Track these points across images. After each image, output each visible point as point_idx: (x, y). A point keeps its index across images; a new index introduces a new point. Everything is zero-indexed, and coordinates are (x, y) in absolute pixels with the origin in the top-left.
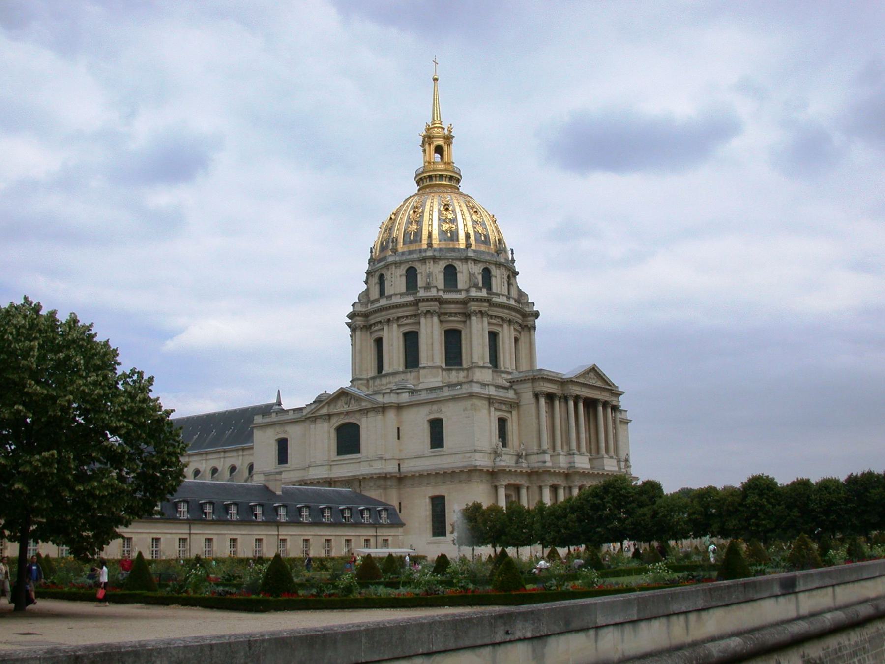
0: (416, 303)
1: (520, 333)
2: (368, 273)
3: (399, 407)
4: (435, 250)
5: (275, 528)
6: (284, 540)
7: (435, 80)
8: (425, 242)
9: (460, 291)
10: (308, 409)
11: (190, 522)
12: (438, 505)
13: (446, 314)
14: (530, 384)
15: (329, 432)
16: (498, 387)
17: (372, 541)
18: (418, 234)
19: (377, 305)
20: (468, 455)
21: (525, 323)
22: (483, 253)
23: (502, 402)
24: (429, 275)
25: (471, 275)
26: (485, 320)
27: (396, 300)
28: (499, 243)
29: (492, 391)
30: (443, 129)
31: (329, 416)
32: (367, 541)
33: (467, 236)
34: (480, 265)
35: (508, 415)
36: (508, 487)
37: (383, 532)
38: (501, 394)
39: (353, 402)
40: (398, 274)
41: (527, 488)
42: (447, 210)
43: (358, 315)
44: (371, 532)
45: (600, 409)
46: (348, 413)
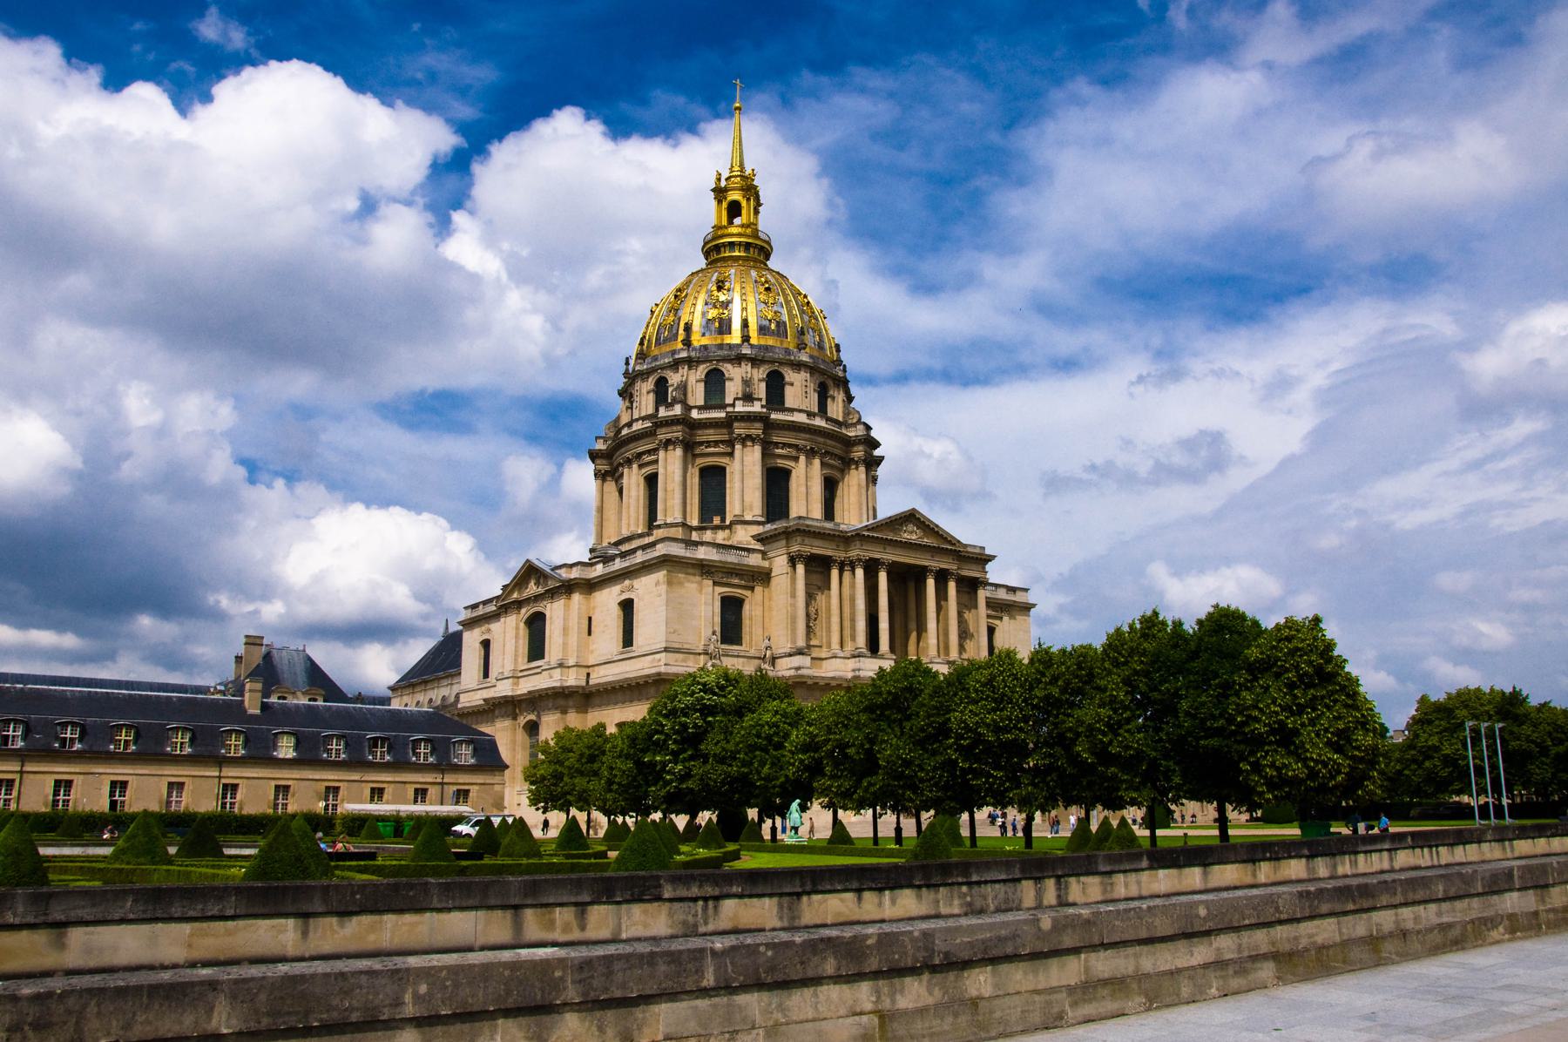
6: (235, 787)
8: (681, 335)
9: (723, 406)
11: (22, 756)
13: (701, 443)
17: (433, 792)
18: (673, 329)
22: (767, 348)
24: (683, 387)
26: (757, 449)
27: (637, 426)
33: (745, 324)
35: (747, 593)
40: (644, 391)
45: (931, 583)
46: (537, 598)
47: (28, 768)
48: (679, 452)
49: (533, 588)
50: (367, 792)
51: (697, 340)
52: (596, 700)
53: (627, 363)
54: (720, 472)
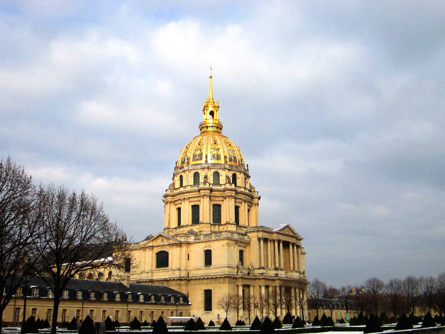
0: (199, 191)
2: (174, 175)
3: (188, 244)
4: (209, 164)
5: (126, 305)
6: (130, 311)
9: (221, 185)
10: (142, 243)
12: (208, 294)
16: (239, 234)
17: (175, 313)
18: (201, 155)
19: (178, 191)
20: (224, 269)
21: (253, 202)
23: (242, 242)
24: (206, 177)
25: (227, 177)
26: (233, 200)
27: (188, 189)
28: (241, 161)
29: (236, 236)
30: (214, 102)
31: (153, 247)
32: (172, 312)
33: (225, 157)
36: (244, 286)
37: (181, 308)
41: (254, 286)
43: (169, 196)
44: (174, 308)
45: (291, 247)
47: (84, 306)
48: (208, 199)
49: (159, 242)
50: (160, 312)
51: (210, 161)
52: (193, 282)
53: (176, 164)
54: (220, 206)
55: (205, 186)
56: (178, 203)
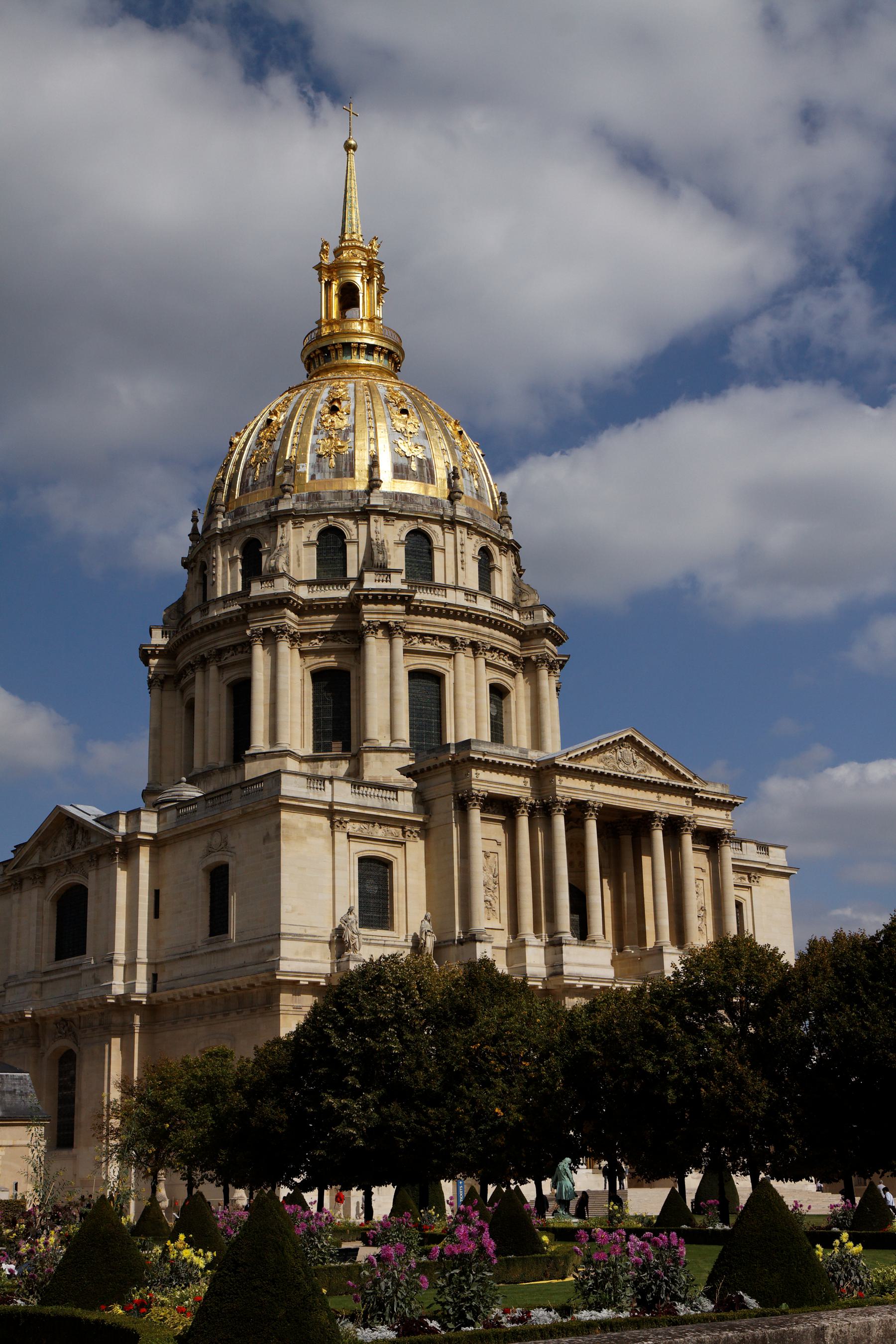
1: (514, 675)
7: (348, 147)
9: (345, 583)
13: (313, 635)
14: (449, 776)
15: (40, 909)
21: (526, 654)
22: (405, 498)
23: (373, 820)
26: (400, 643)
34: (400, 524)
38: (370, 802)
39: (79, 837)
42: (334, 410)
43: (154, 656)
45: (658, 835)
55: (270, 591)
56: (187, 679)
